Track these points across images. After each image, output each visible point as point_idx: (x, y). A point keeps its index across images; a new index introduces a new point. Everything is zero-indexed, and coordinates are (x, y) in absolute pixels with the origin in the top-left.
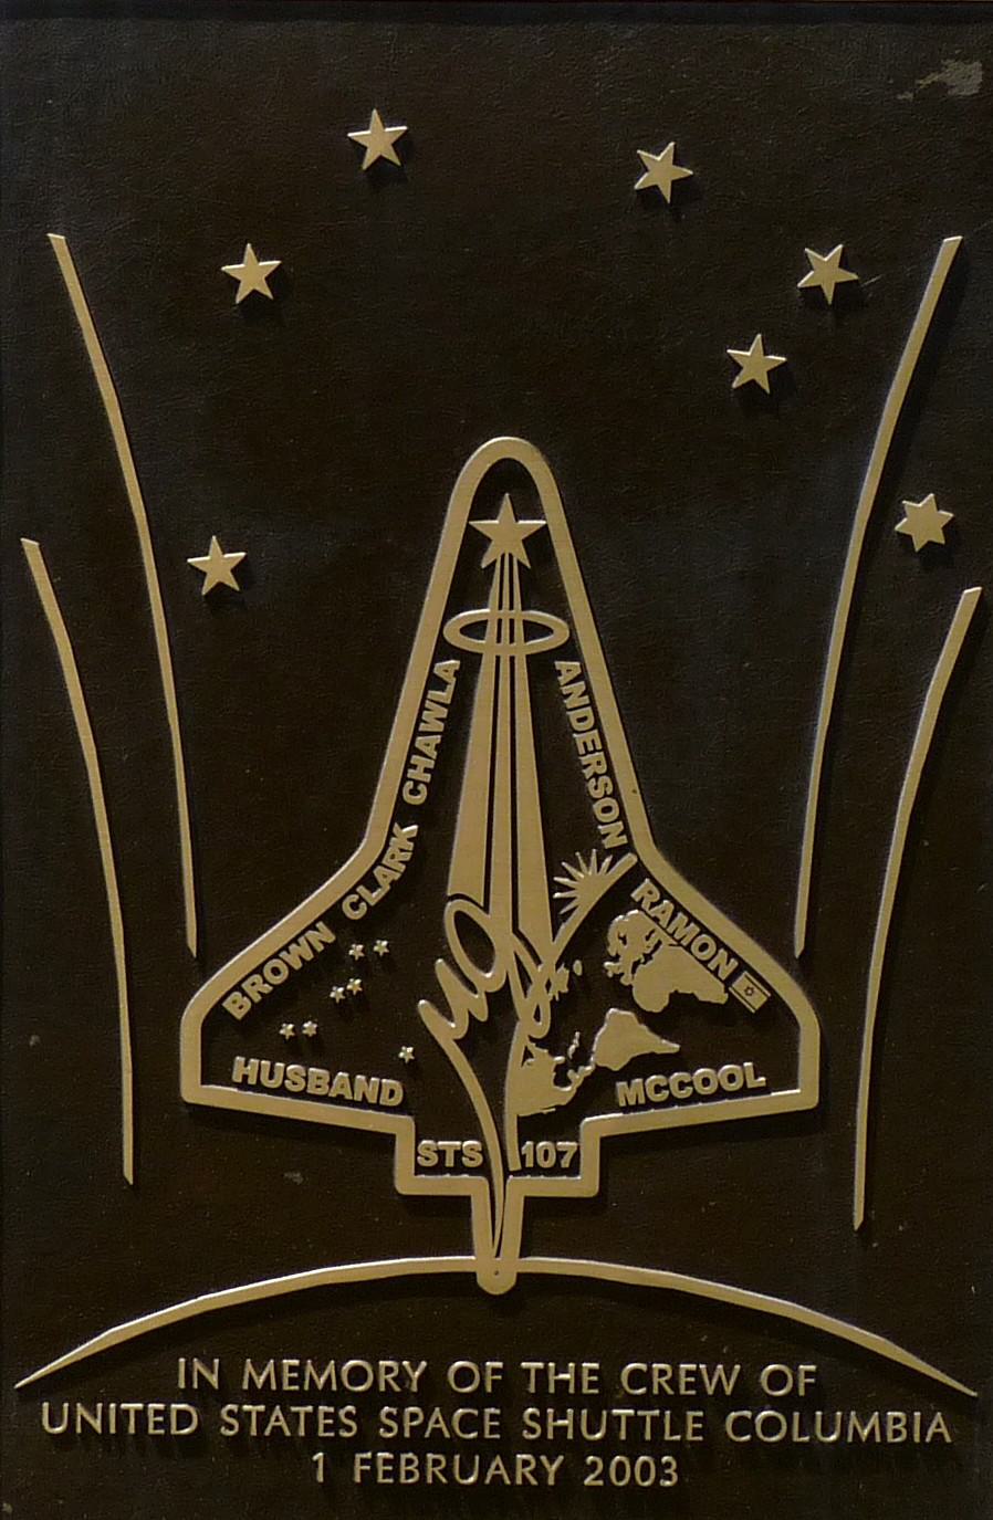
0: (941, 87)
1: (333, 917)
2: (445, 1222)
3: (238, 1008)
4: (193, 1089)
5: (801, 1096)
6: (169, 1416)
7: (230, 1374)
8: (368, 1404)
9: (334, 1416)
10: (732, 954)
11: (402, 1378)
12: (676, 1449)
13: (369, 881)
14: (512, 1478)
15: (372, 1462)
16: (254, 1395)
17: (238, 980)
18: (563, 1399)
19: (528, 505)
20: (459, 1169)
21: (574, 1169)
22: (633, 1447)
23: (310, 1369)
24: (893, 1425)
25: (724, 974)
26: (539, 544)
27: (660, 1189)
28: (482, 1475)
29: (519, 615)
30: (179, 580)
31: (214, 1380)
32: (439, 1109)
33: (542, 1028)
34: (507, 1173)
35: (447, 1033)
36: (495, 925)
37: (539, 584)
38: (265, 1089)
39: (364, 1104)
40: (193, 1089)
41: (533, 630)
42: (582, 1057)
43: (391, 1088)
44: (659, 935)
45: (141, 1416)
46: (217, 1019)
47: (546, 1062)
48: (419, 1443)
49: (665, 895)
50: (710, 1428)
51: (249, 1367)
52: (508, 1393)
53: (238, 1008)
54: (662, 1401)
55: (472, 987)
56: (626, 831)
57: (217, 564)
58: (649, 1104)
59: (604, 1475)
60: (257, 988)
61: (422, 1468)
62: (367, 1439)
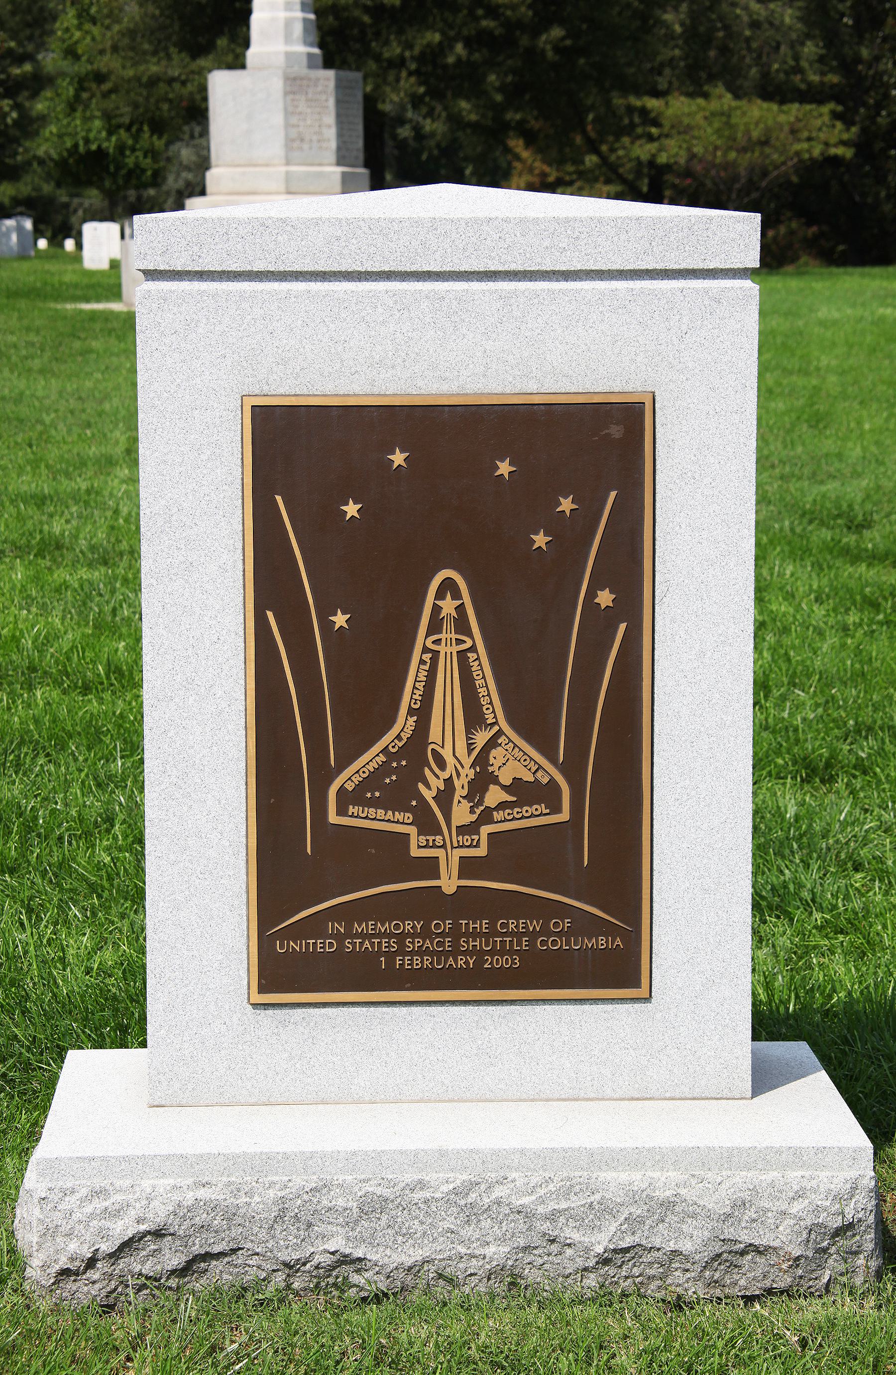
0: (608, 435)
1: (385, 751)
2: (430, 868)
3: (350, 786)
4: (333, 818)
5: (564, 816)
6: (325, 946)
7: (349, 927)
10: (536, 762)
13: (398, 737)
17: (348, 778)
18: (475, 935)
19: (456, 595)
20: (434, 846)
21: (477, 846)
24: (602, 942)
25: (534, 769)
26: (461, 609)
27: (509, 855)
28: (445, 963)
29: (454, 636)
30: (326, 626)
32: (427, 824)
33: (465, 792)
34: (452, 847)
35: (428, 795)
36: (447, 753)
37: (462, 625)
38: (361, 818)
39: (398, 822)
40: (333, 818)
41: (459, 642)
42: (481, 802)
43: (409, 817)
44: (508, 756)
46: (341, 790)
47: (466, 805)
48: (421, 952)
49: (510, 741)
50: (532, 943)
52: (455, 933)
53: (350, 786)
55: (437, 777)
56: (495, 717)
57: (340, 620)
58: (506, 820)
60: (357, 779)
61: (422, 962)
62: (401, 952)
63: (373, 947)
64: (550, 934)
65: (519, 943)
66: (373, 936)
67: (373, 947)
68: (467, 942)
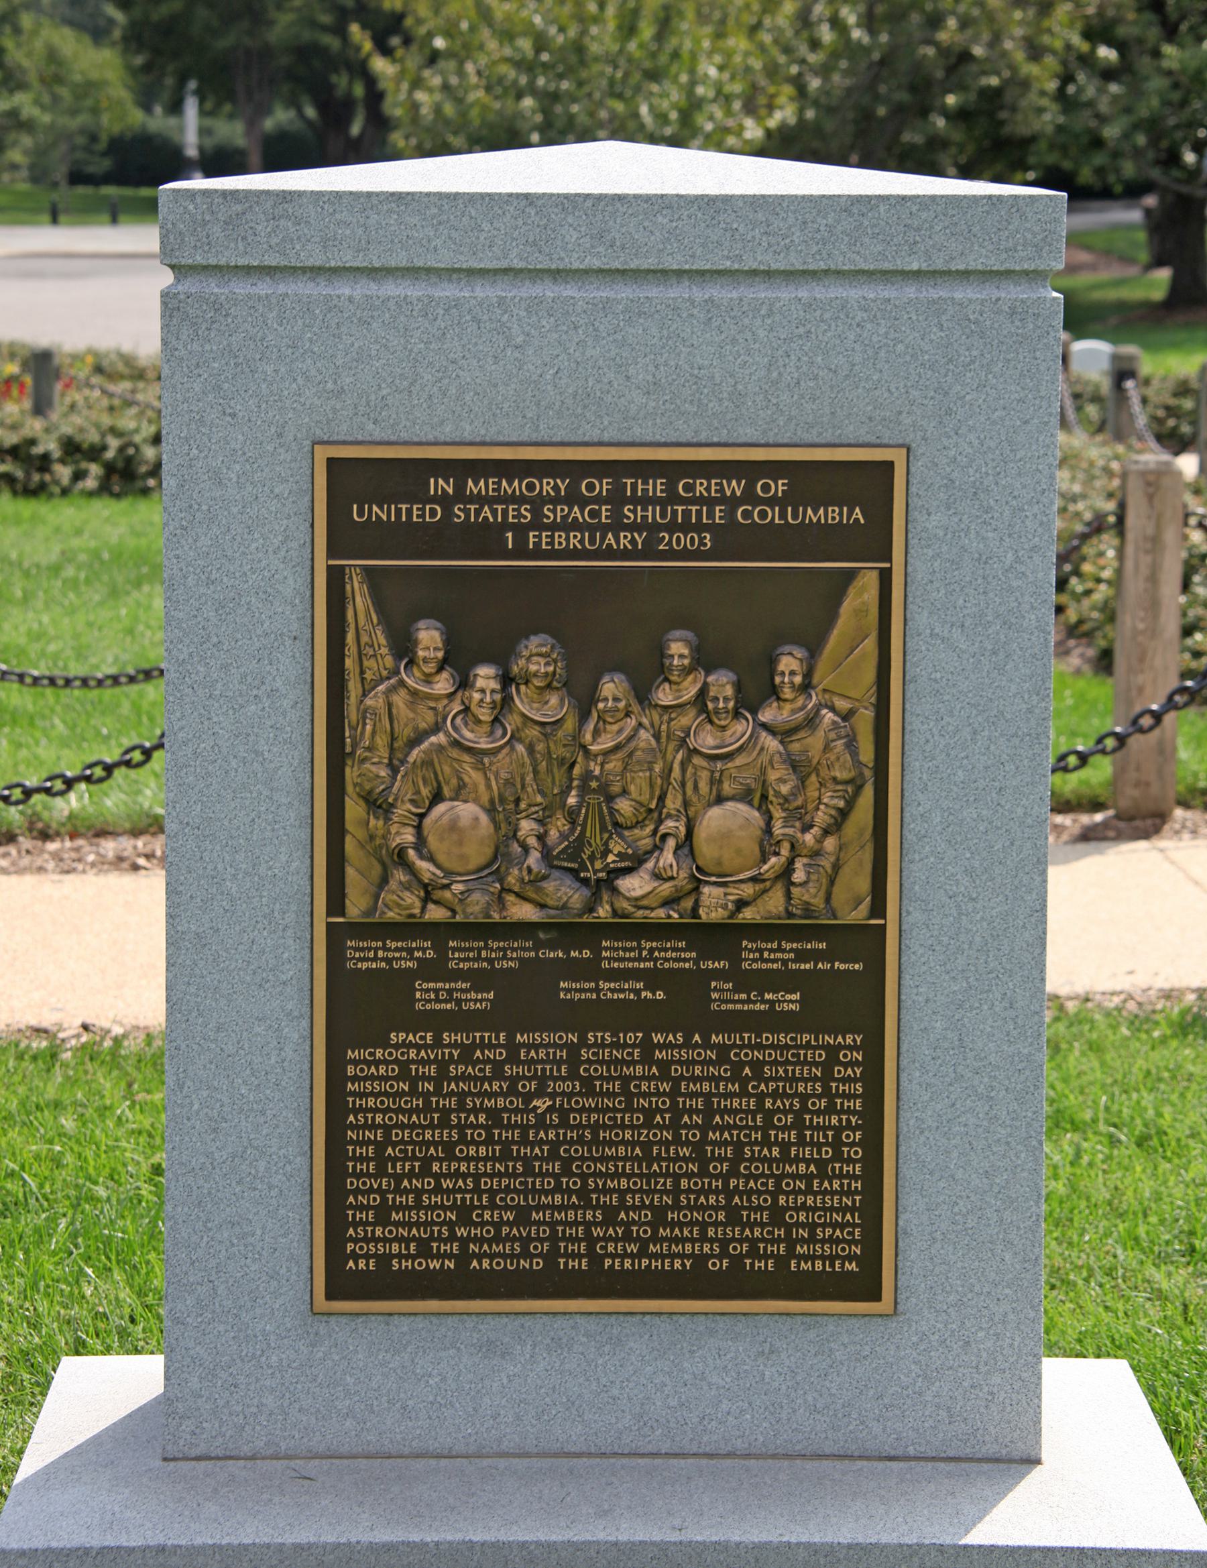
8: (537, 504)
9: (518, 510)
11: (556, 488)
12: (707, 528)
14: (618, 543)
15: (540, 537)
16: (472, 499)
18: (645, 501)
22: (686, 527)
23: (504, 483)
31: (451, 491)
45: (409, 511)
51: (470, 483)
52: (617, 499)
54: (700, 501)
59: (670, 543)
61: (567, 539)
62: (537, 524)
63: (495, 517)
64: (754, 500)
65: (711, 515)
66: (498, 500)
67: (495, 517)
68: (634, 512)
